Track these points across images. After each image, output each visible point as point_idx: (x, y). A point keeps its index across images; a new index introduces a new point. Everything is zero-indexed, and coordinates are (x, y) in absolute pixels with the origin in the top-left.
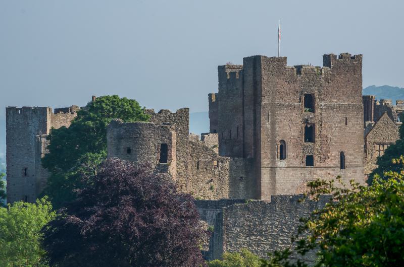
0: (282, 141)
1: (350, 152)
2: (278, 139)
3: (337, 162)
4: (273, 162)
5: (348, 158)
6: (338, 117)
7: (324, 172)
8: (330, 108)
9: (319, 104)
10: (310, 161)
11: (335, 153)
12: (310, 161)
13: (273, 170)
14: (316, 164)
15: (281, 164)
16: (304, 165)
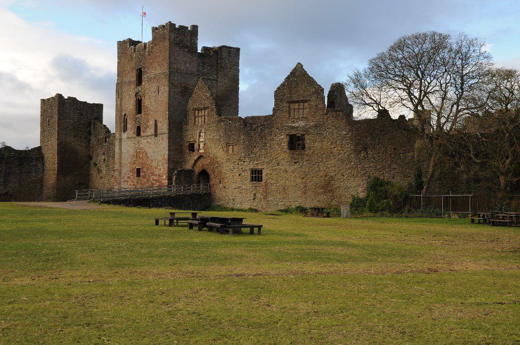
0: (125, 115)
1: (161, 120)
2: (123, 114)
3: (152, 131)
4: (121, 135)
5: (159, 125)
6: (154, 87)
7: (145, 141)
8: (150, 79)
9: (145, 77)
10: (138, 133)
11: (152, 123)
12: (138, 133)
13: (121, 139)
14: (142, 134)
15: (125, 136)
16: (135, 136)
